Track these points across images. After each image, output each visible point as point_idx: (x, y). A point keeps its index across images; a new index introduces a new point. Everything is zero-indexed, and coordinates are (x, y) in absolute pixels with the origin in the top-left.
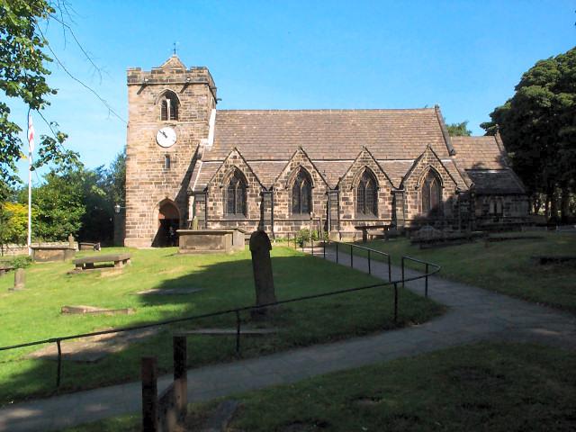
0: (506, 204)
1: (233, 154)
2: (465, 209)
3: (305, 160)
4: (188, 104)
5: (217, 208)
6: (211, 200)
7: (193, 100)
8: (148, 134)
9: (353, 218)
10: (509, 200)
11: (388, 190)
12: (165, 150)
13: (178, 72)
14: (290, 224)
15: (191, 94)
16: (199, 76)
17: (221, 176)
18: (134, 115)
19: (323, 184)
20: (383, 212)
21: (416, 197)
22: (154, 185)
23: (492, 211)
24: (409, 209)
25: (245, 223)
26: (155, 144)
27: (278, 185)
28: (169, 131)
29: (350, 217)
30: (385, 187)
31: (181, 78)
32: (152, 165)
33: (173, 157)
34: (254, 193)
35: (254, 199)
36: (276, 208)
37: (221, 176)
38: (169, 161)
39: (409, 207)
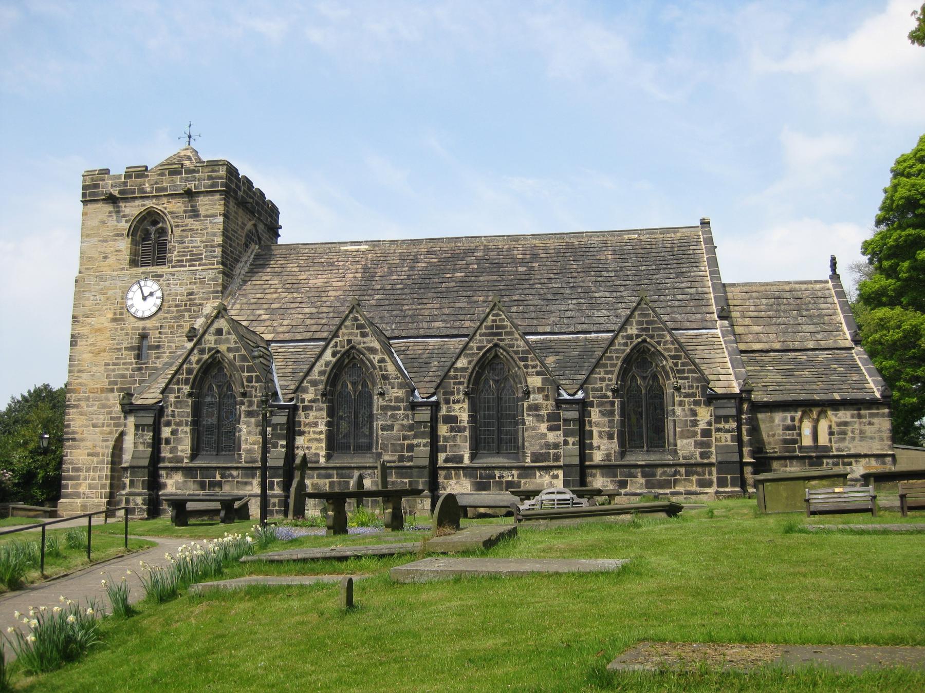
0: (839, 424)
1: (216, 325)
2: (726, 439)
5: (179, 441)
6: (168, 424)
8: (110, 293)
9: (466, 461)
10: (845, 415)
11: (546, 398)
12: (141, 324)
13: (174, 172)
16: (210, 178)
18: (92, 260)
19: (401, 386)
20: (536, 449)
21: (612, 413)
23: (807, 441)
24: (596, 441)
25: (235, 473)
26: (121, 314)
27: (305, 391)
28: (150, 286)
29: (460, 459)
30: (541, 390)
31: (180, 183)
32: (115, 355)
33: (153, 337)
36: (300, 441)
37: (189, 371)
38: (142, 346)
39: (595, 434)
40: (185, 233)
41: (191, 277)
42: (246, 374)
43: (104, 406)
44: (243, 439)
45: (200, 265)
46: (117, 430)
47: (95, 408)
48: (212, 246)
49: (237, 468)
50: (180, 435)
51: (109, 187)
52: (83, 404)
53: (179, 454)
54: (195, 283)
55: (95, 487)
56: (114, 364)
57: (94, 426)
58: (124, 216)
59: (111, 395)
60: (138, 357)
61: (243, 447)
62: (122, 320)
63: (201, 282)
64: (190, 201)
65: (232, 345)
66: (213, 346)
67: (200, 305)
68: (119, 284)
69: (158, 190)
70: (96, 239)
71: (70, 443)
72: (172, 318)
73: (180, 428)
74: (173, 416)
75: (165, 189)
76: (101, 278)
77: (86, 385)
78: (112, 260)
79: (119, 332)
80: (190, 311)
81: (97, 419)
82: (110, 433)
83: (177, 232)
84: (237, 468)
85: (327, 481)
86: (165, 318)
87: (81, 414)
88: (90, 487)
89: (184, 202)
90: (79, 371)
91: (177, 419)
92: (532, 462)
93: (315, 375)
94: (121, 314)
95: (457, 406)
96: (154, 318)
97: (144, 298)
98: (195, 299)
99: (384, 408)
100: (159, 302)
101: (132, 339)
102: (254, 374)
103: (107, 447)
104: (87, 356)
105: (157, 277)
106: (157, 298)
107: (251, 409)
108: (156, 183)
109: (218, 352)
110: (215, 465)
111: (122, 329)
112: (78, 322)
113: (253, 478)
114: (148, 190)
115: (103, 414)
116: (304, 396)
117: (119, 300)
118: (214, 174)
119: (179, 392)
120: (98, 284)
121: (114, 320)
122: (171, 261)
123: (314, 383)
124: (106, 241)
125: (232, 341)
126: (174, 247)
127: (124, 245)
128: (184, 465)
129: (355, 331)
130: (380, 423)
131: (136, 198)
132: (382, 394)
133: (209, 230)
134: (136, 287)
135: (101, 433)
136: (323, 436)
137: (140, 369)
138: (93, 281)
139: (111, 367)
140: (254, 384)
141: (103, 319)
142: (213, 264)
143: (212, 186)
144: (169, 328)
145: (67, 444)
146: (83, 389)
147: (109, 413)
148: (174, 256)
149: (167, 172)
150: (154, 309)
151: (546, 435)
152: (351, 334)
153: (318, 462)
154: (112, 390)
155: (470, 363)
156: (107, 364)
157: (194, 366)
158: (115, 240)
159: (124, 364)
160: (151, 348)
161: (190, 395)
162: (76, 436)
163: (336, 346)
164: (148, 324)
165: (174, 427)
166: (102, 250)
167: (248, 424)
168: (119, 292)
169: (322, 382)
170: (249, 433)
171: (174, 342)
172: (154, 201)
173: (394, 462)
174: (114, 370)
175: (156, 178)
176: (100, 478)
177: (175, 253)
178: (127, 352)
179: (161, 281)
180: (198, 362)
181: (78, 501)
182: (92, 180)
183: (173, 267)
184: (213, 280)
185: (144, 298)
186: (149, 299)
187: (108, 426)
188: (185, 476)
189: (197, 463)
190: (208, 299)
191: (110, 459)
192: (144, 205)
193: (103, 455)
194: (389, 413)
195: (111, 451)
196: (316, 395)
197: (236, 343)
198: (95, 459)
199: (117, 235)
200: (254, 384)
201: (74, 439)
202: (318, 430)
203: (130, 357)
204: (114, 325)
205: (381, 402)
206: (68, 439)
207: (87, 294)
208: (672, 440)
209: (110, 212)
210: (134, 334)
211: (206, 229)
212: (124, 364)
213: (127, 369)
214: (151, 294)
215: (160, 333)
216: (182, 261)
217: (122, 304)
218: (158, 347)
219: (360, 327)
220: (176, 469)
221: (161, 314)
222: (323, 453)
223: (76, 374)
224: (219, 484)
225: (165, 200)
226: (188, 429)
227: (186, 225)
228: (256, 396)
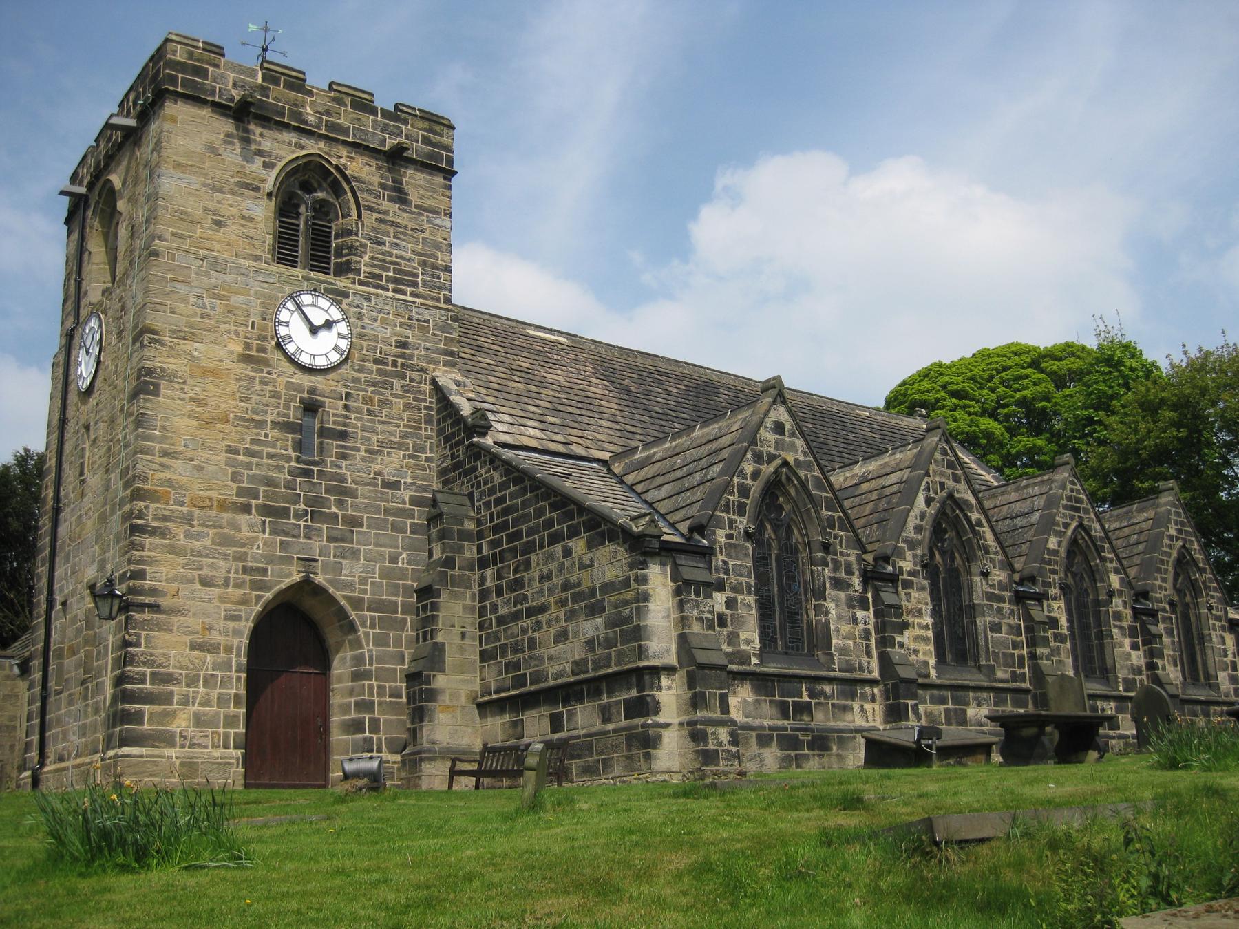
3: (956, 479)
4: (369, 224)
7: (404, 219)
12: (306, 380)
14: (943, 701)
15: (401, 197)
16: (426, 141)
17: (744, 491)
22: (255, 518)
25: (828, 689)
26: (266, 349)
28: (321, 309)
33: (333, 411)
34: (842, 574)
35: (842, 595)
40: (383, 227)
41: (401, 311)
42: (824, 512)
43: (226, 541)
44: (832, 627)
45: (413, 295)
46: (258, 598)
47: (207, 542)
48: (435, 267)
49: (830, 680)
50: (742, 611)
51: (227, 82)
52: (177, 529)
53: (743, 647)
54: (410, 327)
55: (212, 723)
56: (248, 453)
57: (205, 582)
58: (260, 153)
59: (242, 519)
60: (299, 446)
61: (834, 642)
62: (266, 362)
63: (421, 328)
64: (389, 170)
65: (802, 458)
66: (772, 450)
67: (423, 370)
68: (256, 287)
69: (332, 127)
70: (195, 179)
71: (147, 615)
72: (370, 383)
73: (740, 597)
74: (726, 572)
75: (345, 131)
76: (215, 264)
77: (181, 487)
78: (232, 231)
79: (258, 387)
80: (403, 377)
81: (212, 566)
82: (244, 602)
83: (370, 218)
84: (830, 680)
85: (942, 707)
86: (355, 380)
87: (173, 550)
88: (198, 721)
89: (378, 167)
90: (165, 454)
91: (734, 579)
92: (1126, 690)
93: (909, 532)
94: (262, 349)
95: (1055, 605)
96: (331, 376)
97: (314, 330)
98: (411, 357)
99: (990, 597)
100: (344, 344)
101: (287, 407)
102: (836, 515)
103: (237, 633)
104: (183, 424)
105: (337, 296)
106: (340, 336)
107: (837, 575)
108: (327, 113)
109: (785, 463)
110: (803, 672)
111: (264, 382)
112: (162, 344)
113: (853, 700)
114: (311, 119)
115: (225, 557)
116: (901, 563)
117: (258, 321)
118: (434, 138)
119: (730, 527)
120: (207, 275)
121: (246, 359)
122: (358, 272)
123: (912, 544)
124: (221, 191)
125: (800, 450)
126: (364, 246)
127: (262, 212)
128: (752, 668)
129: (945, 469)
130: (988, 619)
131: (286, 126)
132: (985, 574)
133: (427, 235)
134: (290, 305)
135: (223, 599)
136: (930, 634)
137: (307, 473)
138: (196, 265)
139: (241, 458)
140: (836, 531)
141: (220, 352)
142: (438, 300)
143: (431, 156)
144: (365, 401)
145: (137, 616)
146: (174, 495)
147: (241, 557)
148: (364, 262)
149: (348, 100)
150: (335, 357)
151: (1130, 655)
152: (942, 474)
153: (927, 676)
154: (246, 509)
155: (1059, 543)
156: (231, 450)
157: (749, 481)
158: (241, 195)
159: (271, 456)
160: (323, 432)
161: (748, 535)
162: (160, 601)
163: (927, 489)
164: (320, 383)
165: (730, 594)
166: (212, 205)
167: (836, 600)
168: (255, 304)
169: (919, 543)
170: (840, 617)
171: (375, 432)
172: (321, 145)
173: (1006, 681)
174: (248, 466)
175: (326, 102)
176: (222, 701)
177: (366, 258)
178: (276, 433)
179: (344, 306)
180: (755, 475)
181: (173, 752)
182: (191, 55)
183: (361, 283)
184: (443, 329)
185: (314, 330)
186: (323, 334)
187: (237, 586)
188: (757, 690)
189: (772, 668)
190: (436, 362)
191: (244, 660)
192: (300, 146)
193: (228, 650)
194: (996, 605)
195: (246, 642)
196: (915, 564)
197: (805, 454)
198: (209, 658)
199: (246, 186)
200: (836, 531)
201: (155, 608)
202: (924, 622)
203: (285, 445)
204: (247, 370)
205: (986, 589)
206: (142, 606)
207: (181, 289)
208: (1212, 672)
209: (228, 135)
210: (293, 398)
211: (422, 231)
212: (271, 456)
213: (279, 469)
214: (329, 325)
215: (346, 407)
216: (380, 277)
217: (264, 329)
218: (343, 435)
219: (951, 465)
220: (742, 676)
221: (345, 371)
222: (932, 662)
223: (158, 459)
224: (806, 709)
225: (344, 152)
226: (751, 600)
227: (386, 212)
228: (842, 554)
